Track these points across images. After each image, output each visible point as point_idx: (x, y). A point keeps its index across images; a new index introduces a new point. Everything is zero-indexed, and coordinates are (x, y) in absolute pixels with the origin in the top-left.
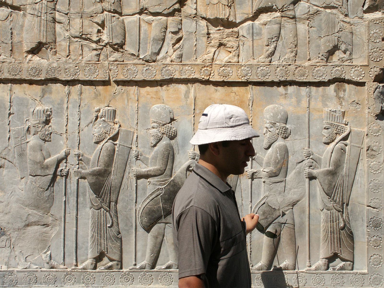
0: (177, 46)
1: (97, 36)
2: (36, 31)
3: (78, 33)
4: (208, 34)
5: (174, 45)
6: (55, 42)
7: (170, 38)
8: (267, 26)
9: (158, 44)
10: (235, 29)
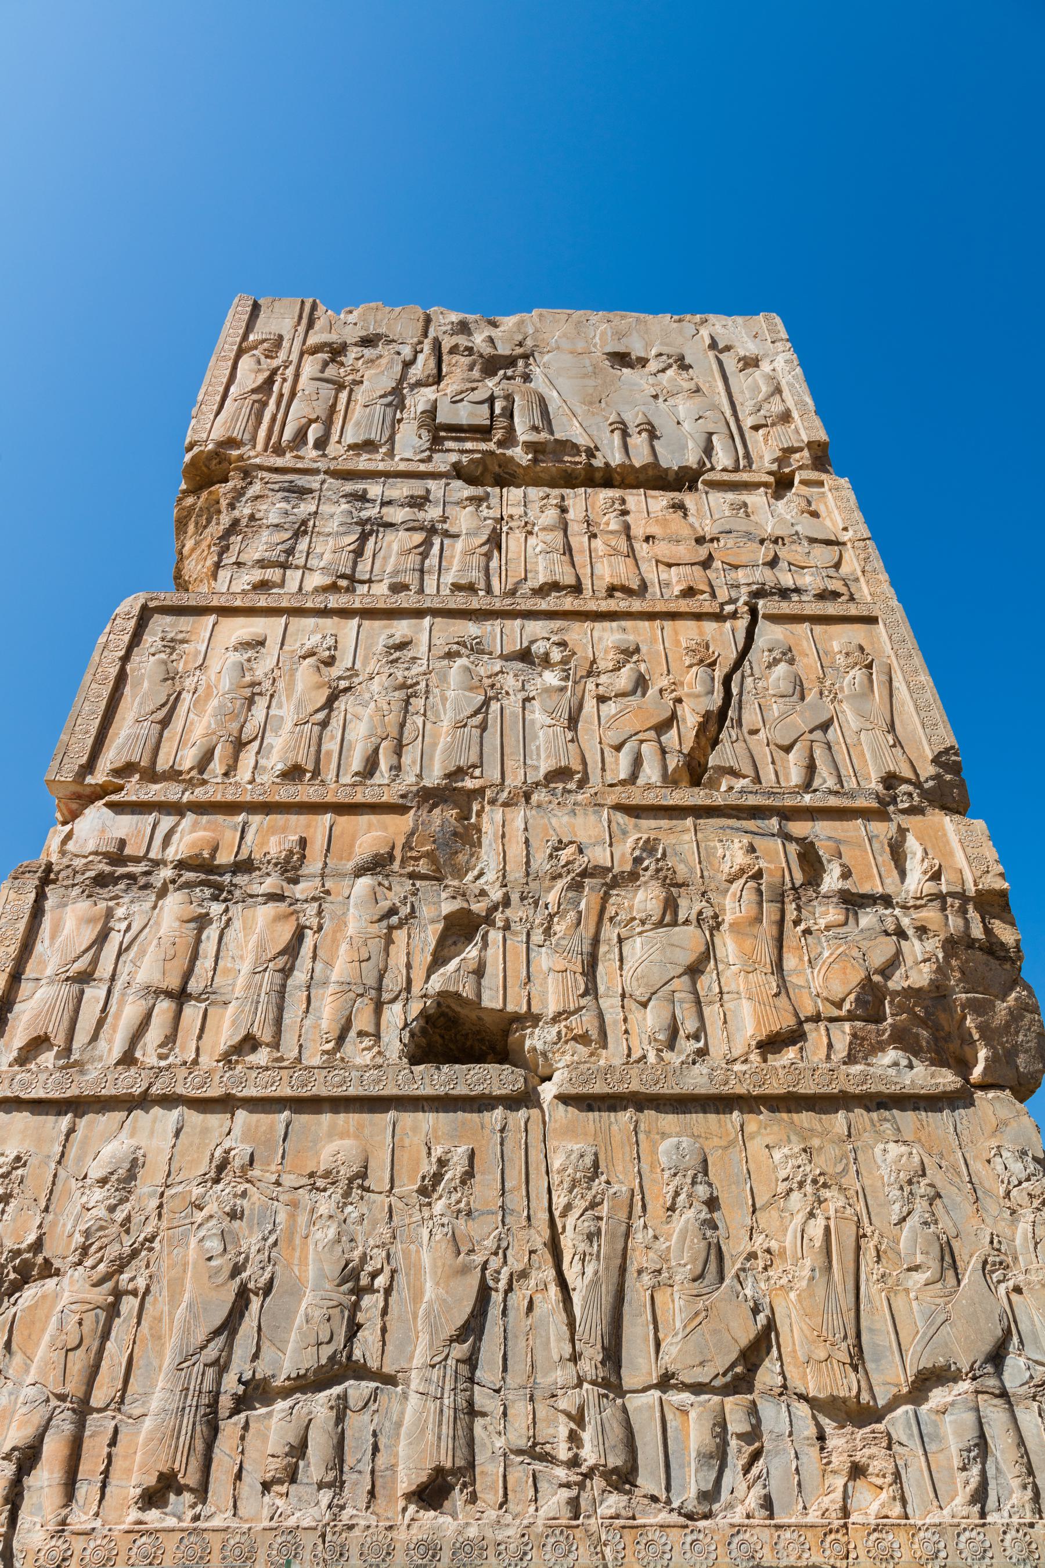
0: (755, 1471)
1: (570, 1449)
2: (430, 1437)
3: (525, 1440)
4: (821, 1437)
5: (747, 1470)
6: (471, 1465)
7: (737, 1453)
8: (948, 1418)
9: (712, 1467)
10: (880, 1427)
